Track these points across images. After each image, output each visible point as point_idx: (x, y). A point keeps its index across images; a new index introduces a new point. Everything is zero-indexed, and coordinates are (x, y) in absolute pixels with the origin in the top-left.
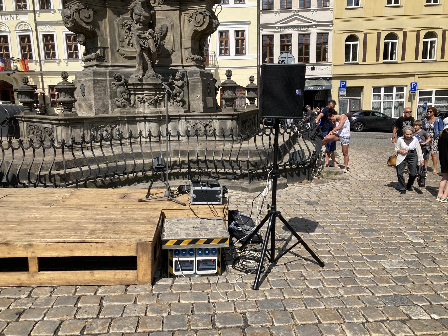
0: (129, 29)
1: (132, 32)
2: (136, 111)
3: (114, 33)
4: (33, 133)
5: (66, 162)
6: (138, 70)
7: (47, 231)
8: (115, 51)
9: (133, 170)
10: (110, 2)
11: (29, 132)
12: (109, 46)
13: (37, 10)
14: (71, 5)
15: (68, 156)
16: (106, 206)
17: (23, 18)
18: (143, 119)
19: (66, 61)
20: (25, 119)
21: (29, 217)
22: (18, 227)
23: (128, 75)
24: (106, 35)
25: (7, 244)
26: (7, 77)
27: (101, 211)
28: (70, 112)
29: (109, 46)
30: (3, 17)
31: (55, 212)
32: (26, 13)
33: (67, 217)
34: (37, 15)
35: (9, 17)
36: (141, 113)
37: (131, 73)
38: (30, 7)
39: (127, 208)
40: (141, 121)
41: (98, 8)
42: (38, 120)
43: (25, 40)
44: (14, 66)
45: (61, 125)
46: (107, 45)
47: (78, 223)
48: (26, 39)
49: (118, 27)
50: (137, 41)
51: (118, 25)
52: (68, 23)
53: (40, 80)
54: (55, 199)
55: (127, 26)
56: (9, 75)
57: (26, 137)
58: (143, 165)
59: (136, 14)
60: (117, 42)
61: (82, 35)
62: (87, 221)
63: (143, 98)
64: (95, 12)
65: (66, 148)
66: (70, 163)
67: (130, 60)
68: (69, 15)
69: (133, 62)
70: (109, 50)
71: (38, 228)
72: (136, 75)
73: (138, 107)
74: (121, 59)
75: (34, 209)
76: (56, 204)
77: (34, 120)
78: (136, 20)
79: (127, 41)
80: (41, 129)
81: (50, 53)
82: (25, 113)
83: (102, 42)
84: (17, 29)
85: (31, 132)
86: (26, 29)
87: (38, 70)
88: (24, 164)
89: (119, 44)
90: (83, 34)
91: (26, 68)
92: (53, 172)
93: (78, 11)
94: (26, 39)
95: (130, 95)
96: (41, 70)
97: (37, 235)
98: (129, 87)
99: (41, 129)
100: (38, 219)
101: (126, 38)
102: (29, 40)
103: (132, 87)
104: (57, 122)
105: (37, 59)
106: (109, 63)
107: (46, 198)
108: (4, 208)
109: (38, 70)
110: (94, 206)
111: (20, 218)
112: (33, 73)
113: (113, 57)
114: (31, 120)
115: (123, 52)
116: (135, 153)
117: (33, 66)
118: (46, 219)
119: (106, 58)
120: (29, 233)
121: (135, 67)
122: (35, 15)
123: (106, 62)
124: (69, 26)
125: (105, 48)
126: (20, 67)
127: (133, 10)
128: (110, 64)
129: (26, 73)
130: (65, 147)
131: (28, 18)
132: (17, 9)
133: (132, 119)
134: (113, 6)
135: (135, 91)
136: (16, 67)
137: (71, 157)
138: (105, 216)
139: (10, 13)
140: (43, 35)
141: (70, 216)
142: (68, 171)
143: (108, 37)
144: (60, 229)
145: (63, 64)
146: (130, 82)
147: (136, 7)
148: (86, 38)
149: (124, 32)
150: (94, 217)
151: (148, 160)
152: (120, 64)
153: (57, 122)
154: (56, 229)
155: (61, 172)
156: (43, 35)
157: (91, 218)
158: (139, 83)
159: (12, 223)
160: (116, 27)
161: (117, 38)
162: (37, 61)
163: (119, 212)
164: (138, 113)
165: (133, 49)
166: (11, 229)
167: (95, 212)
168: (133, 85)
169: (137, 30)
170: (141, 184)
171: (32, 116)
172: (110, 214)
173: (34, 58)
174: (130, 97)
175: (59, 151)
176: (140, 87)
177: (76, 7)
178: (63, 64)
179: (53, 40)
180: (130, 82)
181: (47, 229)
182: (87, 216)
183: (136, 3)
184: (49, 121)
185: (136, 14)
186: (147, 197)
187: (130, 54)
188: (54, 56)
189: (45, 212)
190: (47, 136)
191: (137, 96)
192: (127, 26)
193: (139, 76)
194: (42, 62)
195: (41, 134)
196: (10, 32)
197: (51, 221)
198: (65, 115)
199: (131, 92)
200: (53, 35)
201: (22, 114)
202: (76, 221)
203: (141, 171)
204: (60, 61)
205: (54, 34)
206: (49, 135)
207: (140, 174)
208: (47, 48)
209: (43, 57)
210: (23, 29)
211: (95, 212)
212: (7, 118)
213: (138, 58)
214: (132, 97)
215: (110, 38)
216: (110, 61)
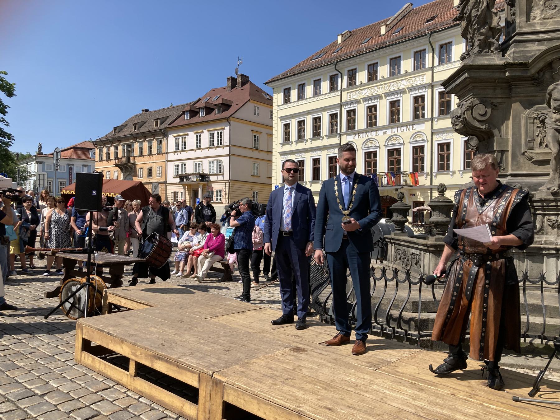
0: (543, 122)
1: (547, 125)
2: (544, 239)
3: (520, 129)
4: (400, 259)
5: (423, 303)
6: (553, 179)
7: (352, 411)
8: (519, 155)
9: (525, 333)
10: (519, 90)
11: (396, 257)
12: (510, 148)
13: (436, 118)
14: (463, 102)
15: (427, 295)
16: (455, 392)
17: (418, 128)
18: (554, 252)
19: (461, 173)
20: (394, 241)
21: (342, 380)
22: (323, 392)
23: (536, 187)
24: (507, 134)
25: (300, 414)
26: (395, 192)
27: (443, 399)
28: (443, 237)
29: (510, 148)
30: (399, 129)
31: (377, 381)
32: (423, 123)
33: (390, 395)
34: (434, 123)
35: (405, 128)
36: (551, 243)
37: (541, 185)
38: (428, 115)
39: (489, 407)
40: (550, 256)
41: (499, 100)
42: (406, 244)
43: (418, 151)
44: (404, 180)
45: (429, 252)
46: (508, 147)
47: (400, 410)
48: (419, 150)
49: (527, 121)
50: (554, 137)
51: (527, 119)
52: (456, 125)
53: (429, 194)
54: (388, 358)
55: (540, 118)
56: (397, 190)
57: (393, 263)
58: (542, 327)
59: (555, 100)
60: (523, 142)
61: (475, 138)
62: (413, 411)
63: (557, 221)
64: (494, 107)
65: (438, 283)
66: (432, 306)
67: (541, 166)
68: (459, 115)
69: (547, 169)
70: (510, 154)
71: (344, 402)
72: (549, 186)
73: (547, 234)
74: (527, 165)
75: (355, 368)
76: (384, 368)
77: (402, 243)
78: (555, 109)
79: (538, 140)
80: (409, 255)
81: (444, 164)
82: (396, 234)
83: (499, 144)
84: (412, 140)
85: (399, 257)
86: (421, 139)
87: (428, 184)
88: (377, 298)
89: (526, 145)
90: (477, 137)
91: (416, 182)
92: (407, 315)
93: (471, 108)
94: (419, 150)
95: (536, 215)
96: (431, 184)
97: (338, 413)
98: (535, 204)
99: (409, 255)
100: (351, 387)
101: (538, 136)
102: (423, 152)
103: (539, 204)
104: (425, 248)
105: (429, 171)
106: (508, 171)
107: (377, 355)
108: (324, 357)
109: (428, 184)
110: (436, 386)
111: (332, 379)
112: (423, 188)
113: (515, 163)
114: (399, 242)
115: (531, 155)
116: (533, 305)
117: (423, 181)
118: (361, 390)
119: (503, 165)
120: (330, 406)
121: (548, 175)
122: (432, 122)
123: (504, 170)
124: (457, 128)
125: (503, 152)
126: (410, 181)
127: (550, 95)
128: (509, 172)
129: (414, 187)
130: (423, 283)
131: (424, 128)
132: (414, 119)
133: (535, 251)
134: (522, 95)
135: (543, 209)
136: (406, 181)
137: (430, 297)
138: (445, 412)
139: (407, 124)
140: (439, 144)
141: (395, 395)
142: (425, 316)
143: (510, 137)
144: (370, 415)
145: (458, 175)
146: (538, 196)
147: (556, 90)
148: (480, 141)
149: (535, 128)
150: (428, 407)
151: (555, 320)
152: (525, 172)
153: (425, 248)
154: (365, 412)
155: (415, 315)
156: (439, 144)
157: (423, 409)
158: (552, 197)
159: (319, 381)
160: (523, 122)
161: (523, 137)
162: (428, 174)
163: (472, 411)
164: (546, 243)
165: (547, 150)
166: (314, 393)
167: (433, 398)
168: (541, 201)
169: (555, 122)
170: (538, 358)
171: (400, 238)
172: (456, 410)
173: (425, 171)
174: (535, 219)
175: (416, 287)
176: (554, 204)
177: (468, 103)
178: (458, 175)
179: (448, 149)
180: (538, 196)
181: (354, 408)
182: (417, 403)
183: (557, 85)
184: (417, 246)
185: (555, 100)
186: (532, 394)
187: (541, 158)
188: (448, 167)
189: (367, 377)
190: (414, 264)
191: (546, 217)
192: (540, 118)
193: (553, 188)
194: (434, 174)
195: (408, 260)
196: (404, 145)
197: (366, 394)
198: (436, 240)
199: (538, 212)
200: (450, 143)
201: (392, 236)
202: (400, 407)
203: (539, 337)
204: (454, 173)
205: (451, 141)
206: (416, 264)
207: (537, 341)
208: (441, 158)
209: (435, 169)
210: (418, 139)
211: (433, 398)
212: (381, 238)
213: (553, 162)
214: (539, 218)
215: (513, 138)
216: (510, 168)
